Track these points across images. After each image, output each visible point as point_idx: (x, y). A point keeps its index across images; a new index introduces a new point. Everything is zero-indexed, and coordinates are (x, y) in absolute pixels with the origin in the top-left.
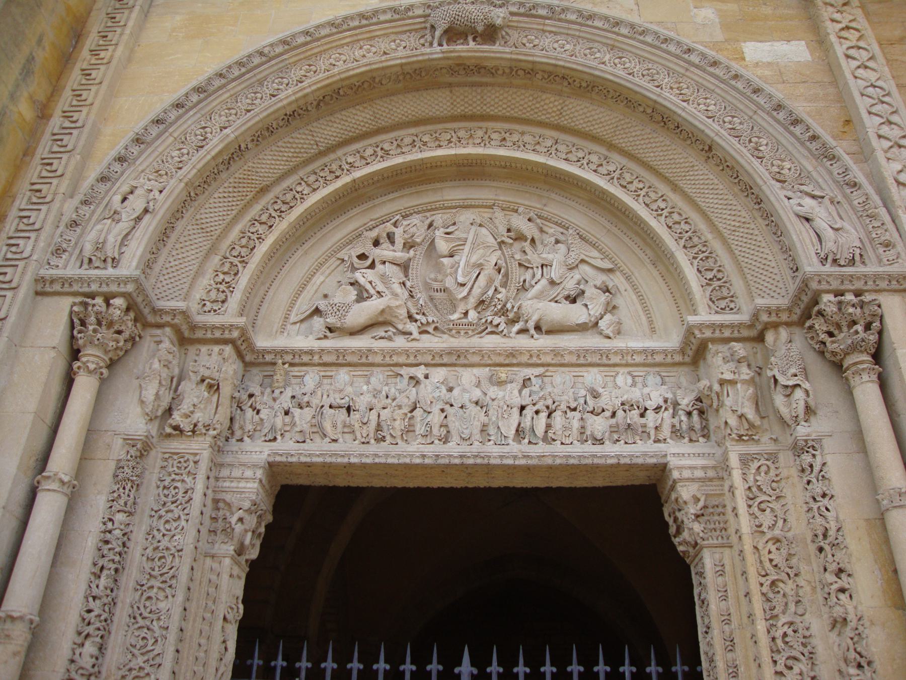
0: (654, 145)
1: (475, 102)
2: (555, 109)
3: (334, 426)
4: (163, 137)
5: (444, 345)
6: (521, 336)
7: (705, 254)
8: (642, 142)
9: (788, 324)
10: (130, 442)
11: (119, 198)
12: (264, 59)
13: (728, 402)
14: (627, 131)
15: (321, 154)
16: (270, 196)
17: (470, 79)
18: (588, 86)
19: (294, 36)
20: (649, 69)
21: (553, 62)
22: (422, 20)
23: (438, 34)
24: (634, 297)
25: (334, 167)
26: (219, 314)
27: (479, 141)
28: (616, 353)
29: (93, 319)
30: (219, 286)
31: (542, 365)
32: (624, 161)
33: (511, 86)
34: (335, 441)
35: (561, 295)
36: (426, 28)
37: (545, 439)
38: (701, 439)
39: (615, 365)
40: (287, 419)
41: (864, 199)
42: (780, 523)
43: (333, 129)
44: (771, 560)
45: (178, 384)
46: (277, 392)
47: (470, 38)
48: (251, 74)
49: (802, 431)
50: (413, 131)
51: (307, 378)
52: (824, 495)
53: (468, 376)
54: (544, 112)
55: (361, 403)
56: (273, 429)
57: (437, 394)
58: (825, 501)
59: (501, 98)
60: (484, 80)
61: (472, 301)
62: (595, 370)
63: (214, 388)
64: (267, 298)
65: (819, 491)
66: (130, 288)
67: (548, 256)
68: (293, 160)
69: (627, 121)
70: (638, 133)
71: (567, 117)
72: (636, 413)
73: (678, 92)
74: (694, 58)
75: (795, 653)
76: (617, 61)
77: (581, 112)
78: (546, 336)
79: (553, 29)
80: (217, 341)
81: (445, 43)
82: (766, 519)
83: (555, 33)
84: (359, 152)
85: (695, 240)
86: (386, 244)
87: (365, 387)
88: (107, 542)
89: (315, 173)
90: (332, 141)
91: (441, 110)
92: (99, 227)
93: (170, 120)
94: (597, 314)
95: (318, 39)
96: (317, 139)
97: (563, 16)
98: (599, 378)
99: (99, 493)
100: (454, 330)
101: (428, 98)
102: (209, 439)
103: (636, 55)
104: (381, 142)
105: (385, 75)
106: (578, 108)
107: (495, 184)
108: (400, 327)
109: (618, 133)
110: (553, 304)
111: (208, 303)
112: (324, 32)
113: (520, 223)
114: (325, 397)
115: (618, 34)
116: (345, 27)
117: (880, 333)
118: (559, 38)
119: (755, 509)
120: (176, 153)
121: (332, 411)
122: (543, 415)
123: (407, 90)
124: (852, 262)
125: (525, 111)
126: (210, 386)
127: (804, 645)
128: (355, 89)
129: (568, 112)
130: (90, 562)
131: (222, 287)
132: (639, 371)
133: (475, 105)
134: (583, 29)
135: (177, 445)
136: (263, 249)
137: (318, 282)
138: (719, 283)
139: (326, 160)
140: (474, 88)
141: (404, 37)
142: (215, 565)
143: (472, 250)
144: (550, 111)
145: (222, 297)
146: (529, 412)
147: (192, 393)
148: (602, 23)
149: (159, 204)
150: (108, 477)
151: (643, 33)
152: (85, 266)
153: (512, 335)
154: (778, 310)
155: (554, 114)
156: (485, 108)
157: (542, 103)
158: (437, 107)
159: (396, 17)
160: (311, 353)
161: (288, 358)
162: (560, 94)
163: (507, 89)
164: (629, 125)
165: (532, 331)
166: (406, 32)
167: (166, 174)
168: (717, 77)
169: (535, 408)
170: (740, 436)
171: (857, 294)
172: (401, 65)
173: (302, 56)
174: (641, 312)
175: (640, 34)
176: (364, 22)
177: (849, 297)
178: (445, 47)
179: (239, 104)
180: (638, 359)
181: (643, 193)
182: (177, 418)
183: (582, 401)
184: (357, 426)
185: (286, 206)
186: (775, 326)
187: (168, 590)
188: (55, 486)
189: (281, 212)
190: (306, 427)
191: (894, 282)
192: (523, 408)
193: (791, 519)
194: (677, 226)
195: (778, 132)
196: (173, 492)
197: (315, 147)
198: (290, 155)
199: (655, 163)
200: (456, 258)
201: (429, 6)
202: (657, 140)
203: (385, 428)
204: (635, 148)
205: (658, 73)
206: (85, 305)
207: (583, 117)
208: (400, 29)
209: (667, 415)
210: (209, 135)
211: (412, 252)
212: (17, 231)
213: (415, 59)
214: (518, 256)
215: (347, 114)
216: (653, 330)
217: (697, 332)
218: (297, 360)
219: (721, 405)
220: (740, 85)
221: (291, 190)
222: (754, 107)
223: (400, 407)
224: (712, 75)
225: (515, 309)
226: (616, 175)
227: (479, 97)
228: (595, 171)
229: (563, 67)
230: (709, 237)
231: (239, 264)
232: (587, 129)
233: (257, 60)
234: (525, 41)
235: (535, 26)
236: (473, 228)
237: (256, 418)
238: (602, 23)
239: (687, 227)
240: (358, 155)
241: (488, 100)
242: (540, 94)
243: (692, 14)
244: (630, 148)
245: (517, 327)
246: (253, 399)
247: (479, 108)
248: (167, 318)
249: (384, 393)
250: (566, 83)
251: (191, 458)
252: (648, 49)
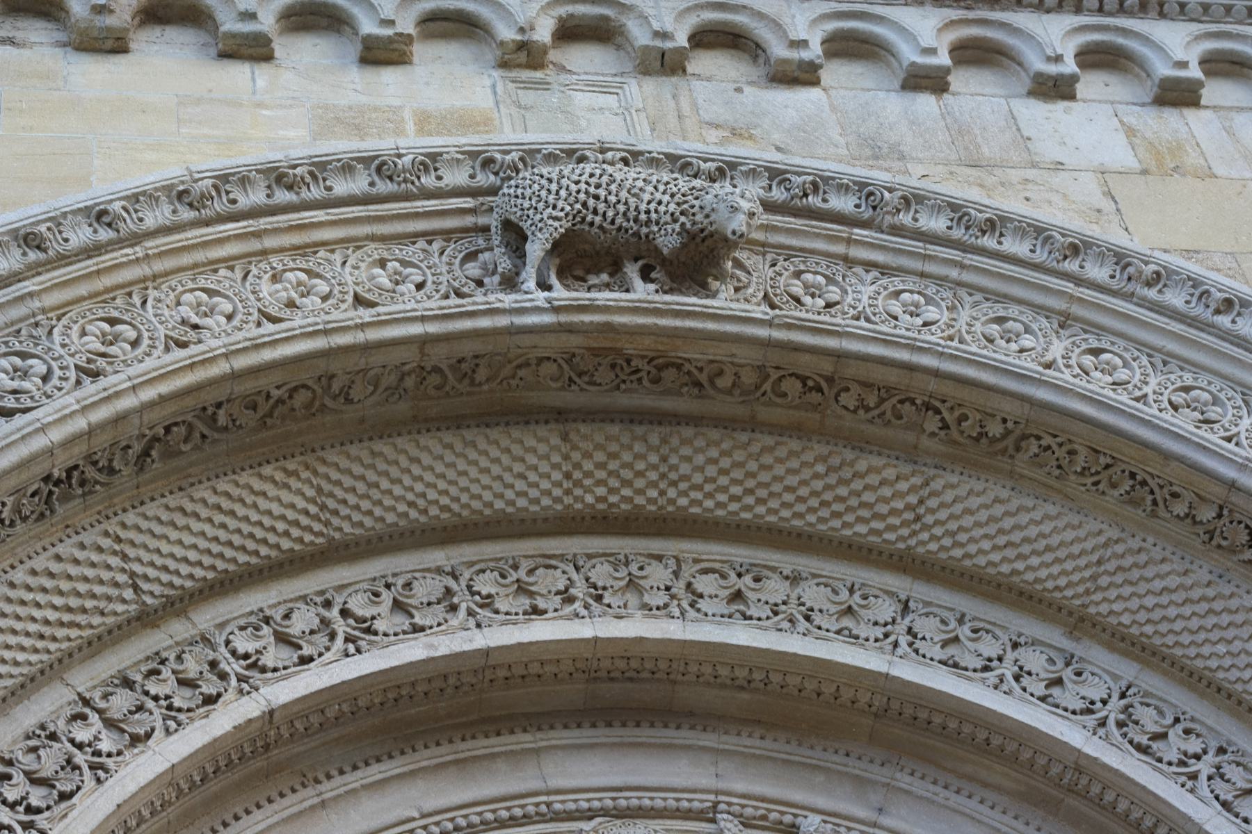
0: (1225, 619)
1: (640, 474)
2: (899, 505)
8: (1187, 610)
14: (1135, 574)
15: (146, 619)
17: (624, 400)
18: (1008, 433)
19: (57, 222)
20: (1187, 389)
21: (904, 356)
22: (468, 203)
25: (192, 667)
27: (660, 598)
32: (1128, 670)
33: (753, 425)
36: (486, 229)
43: (188, 539)
47: (632, 271)
50: (438, 557)
54: (865, 513)
59: (725, 463)
60: (668, 404)
68: (61, 633)
69: (1134, 544)
70: (1172, 582)
71: (938, 531)
76: (1088, 360)
77: (983, 516)
79: (879, 257)
83: (885, 270)
84: (267, 620)
89: (128, 684)
90: (185, 577)
91: (534, 493)
95: (136, 239)
96: (137, 568)
97: (905, 219)
101: (494, 452)
103: (1140, 344)
104: (340, 588)
105: (364, 371)
106: (974, 502)
107: (708, 740)
109: (1104, 581)
112: (152, 219)
115: (1079, 281)
116: (219, 206)
118: (897, 283)
123: (421, 423)
125: (801, 508)
128: (264, 408)
129: (943, 515)
133: (640, 483)
140: (639, 430)
141: (411, 252)
144: (883, 509)
151: (1156, 279)
155: (896, 521)
156: (672, 493)
157: (857, 485)
158: (520, 485)
159: (384, 187)
162: (911, 455)
163: (743, 437)
164: (1143, 558)
166: (414, 237)
172: (424, 342)
173: (82, 290)
175: (1149, 284)
176: (282, 196)
178: (560, 293)
181: (1204, 768)
185: (42, 791)
189: (30, 810)
197: (128, 594)
198: (52, 615)
199: (1234, 674)
201: (488, 163)
202: (1234, 603)
204: (1164, 628)
205: (1216, 401)
207: (992, 529)
213: (467, 324)
215: (236, 492)
221: (53, 737)
226: (1113, 711)
227: (653, 458)
229: (936, 373)
232: (1005, 568)
234: (798, 289)
235: (820, 245)
240: (266, 630)
241: (685, 468)
242: (849, 455)
244: (1149, 629)
247: (653, 493)
250: (932, 424)
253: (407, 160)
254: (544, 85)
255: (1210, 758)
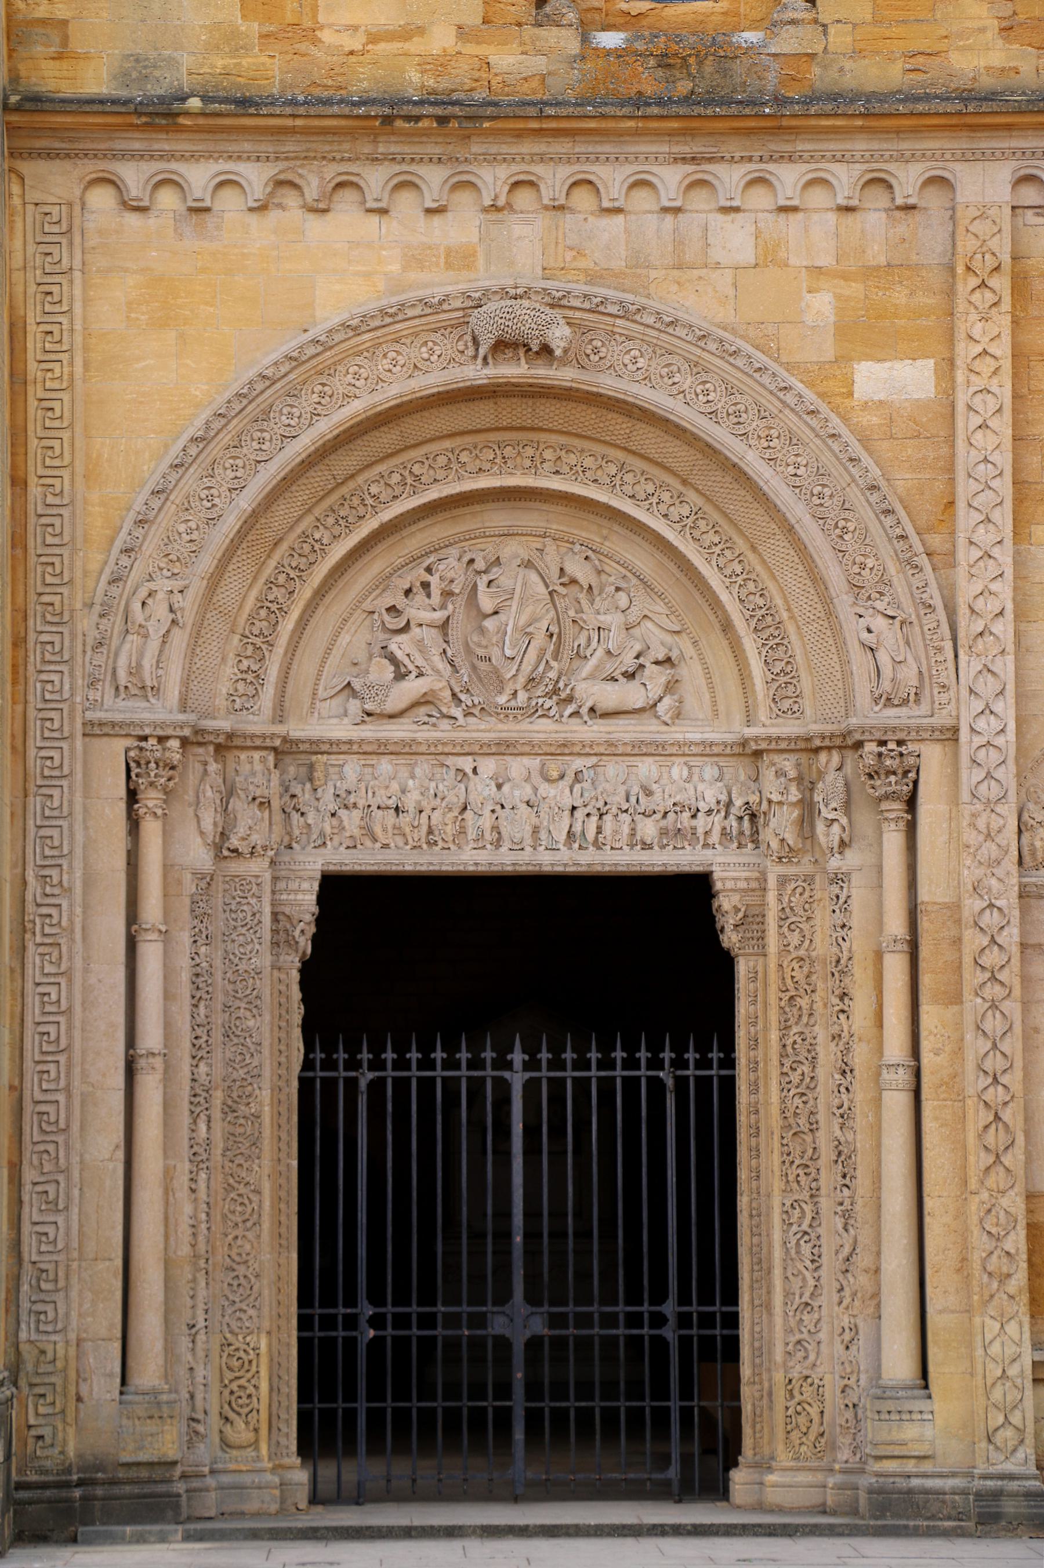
3: (385, 830)
4: (166, 508)
5: (492, 735)
6: (575, 720)
7: (777, 641)
9: (840, 747)
10: (196, 874)
11: (137, 606)
12: (268, 383)
13: (773, 823)
16: (284, 546)
20: (735, 404)
22: (460, 314)
23: (482, 351)
24: (699, 668)
26: (253, 714)
28: (672, 744)
29: (153, 765)
30: (244, 676)
31: (596, 754)
32: (700, 502)
34: (385, 846)
35: (618, 671)
37: (597, 845)
38: (750, 845)
39: (671, 755)
40: (335, 822)
41: (935, 624)
42: (807, 942)
44: (793, 977)
45: (228, 803)
46: (320, 790)
47: (521, 352)
48: (253, 405)
49: (834, 863)
50: (447, 444)
51: (346, 768)
52: (843, 926)
53: (517, 767)
55: (410, 802)
56: (322, 834)
57: (486, 793)
58: (843, 933)
61: (522, 680)
62: (650, 759)
63: (265, 804)
64: (291, 672)
65: (840, 922)
66: (187, 732)
67: (605, 619)
70: (719, 479)
72: (687, 815)
73: (766, 444)
74: (790, 399)
75: (801, 1058)
78: (600, 721)
80: (257, 748)
81: (490, 360)
82: (794, 939)
85: (769, 619)
86: (420, 597)
87: (411, 782)
88: (197, 975)
92: (127, 646)
93: (171, 487)
94: (656, 697)
95: (331, 348)
97: (638, 317)
98: (654, 768)
99: (182, 929)
100: (505, 712)
102: (268, 860)
107: (545, 507)
108: (445, 710)
110: (609, 686)
111: (238, 700)
112: (338, 337)
113: (577, 568)
114: (370, 794)
117: (916, 783)
118: (629, 345)
119: (785, 929)
120: (182, 528)
121: (380, 812)
122: (594, 819)
124: (905, 702)
126: (262, 803)
127: (809, 1051)
130: (188, 995)
131: (250, 677)
132: (695, 761)
134: (663, 336)
135: (236, 867)
136: (288, 625)
137: (344, 644)
138: (787, 679)
139: (344, 490)
142: (283, 976)
143: (519, 612)
145: (251, 691)
146: (579, 814)
147: (246, 816)
148: (685, 332)
149: (187, 613)
150: (186, 914)
152: (123, 696)
153: (564, 720)
154: (832, 736)
159: (429, 311)
160: (350, 742)
161: (325, 747)
165: (586, 718)
166: (439, 328)
167: (179, 560)
168: (813, 429)
169: (586, 811)
170: (780, 858)
171: (900, 743)
174: (705, 689)
176: (388, 320)
177: (892, 746)
179: (245, 450)
180: (694, 749)
181: (717, 550)
182: (234, 842)
183: (633, 800)
184: (407, 830)
185: (304, 560)
186: (829, 748)
187: (255, 1011)
188: (154, 936)
190: (357, 832)
191: (937, 733)
192: (574, 808)
193: (817, 939)
194: (751, 597)
195: (868, 515)
196: (241, 915)
200: (502, 617)
203: (436, 833)
206: (141, 749)
208: (433, 326)
209: (718, 818)
210: (217, 501)
211: (450, 607)
212: (44, 662)
214: (572, 613)
216: (716, 713)
217: (752, 743)
218: (335, 749)
219: (766, 824)
220: (836, 447)
222: (848, 479)
223: (450, 810)
224: (806, 423)
225: (568, 691)
228: (665, 516)
230: (785, 615)
231: (264, 647)
233: (259, 387)
236: (522, 571)
237: (302, 819)
238: (685, 332)
239: (761, 602)
243: (803, 304)
245: (570, 709)
246: (295, 800)
248: (211, 738)
249: (432, 792)
251: (253, 880)
252: (739, 375)
253: (436, 300)
254: (501, 222)
255: (720, 546)
